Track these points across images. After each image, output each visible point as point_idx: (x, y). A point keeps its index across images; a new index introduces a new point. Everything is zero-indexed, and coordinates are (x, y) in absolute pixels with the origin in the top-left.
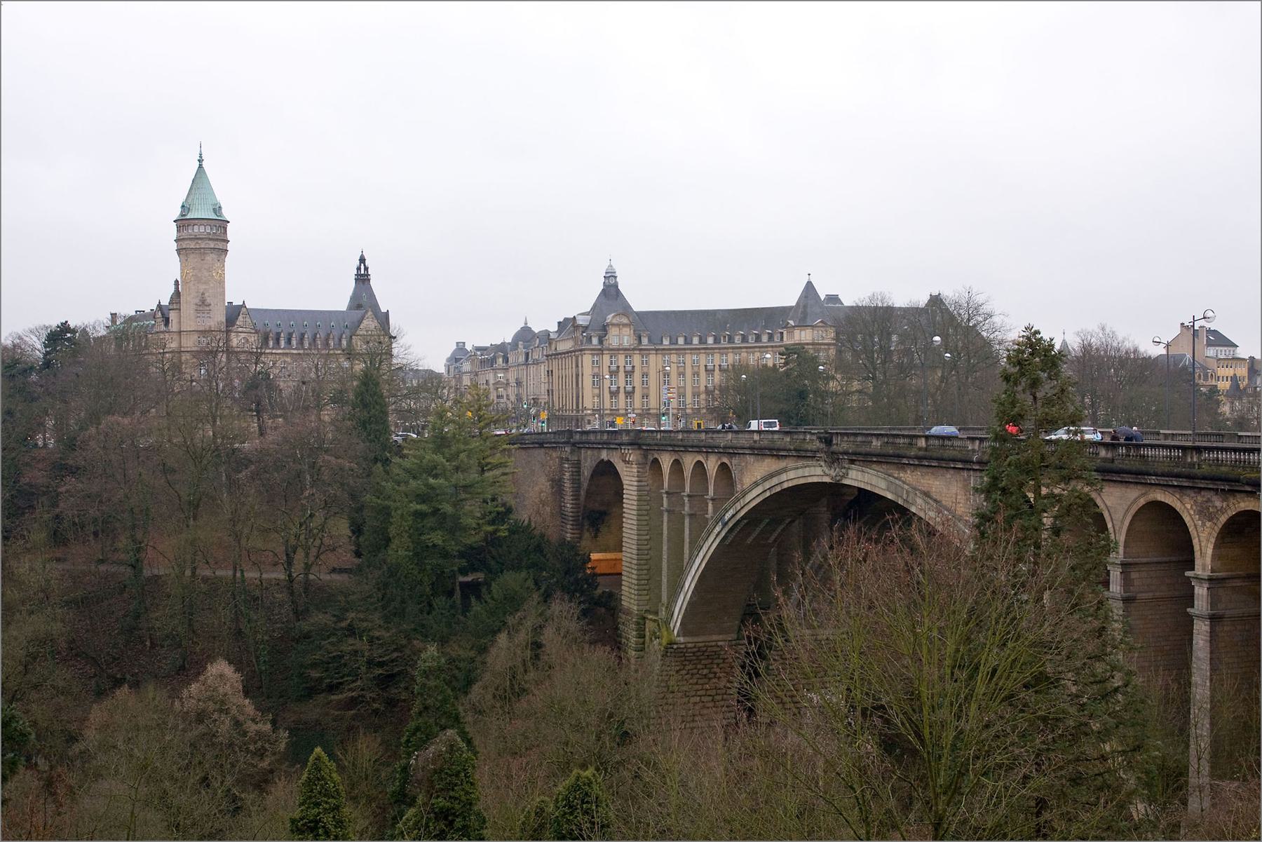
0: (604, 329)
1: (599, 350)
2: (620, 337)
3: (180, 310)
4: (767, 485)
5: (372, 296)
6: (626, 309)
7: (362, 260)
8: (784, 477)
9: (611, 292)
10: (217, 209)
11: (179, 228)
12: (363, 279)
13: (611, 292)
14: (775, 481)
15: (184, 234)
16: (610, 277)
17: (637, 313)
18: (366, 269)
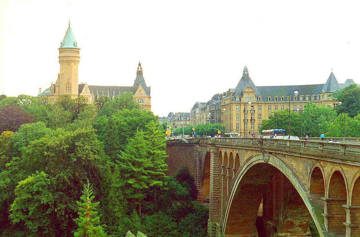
0: (242, 94)
1: (239, 103)
2: (249, 98)
3: (59, 86)
4: (248, 164)
5: (143, 81)
6: (252, 86)
7: (140, 65)
8: (252, 160)
9: (246, 78)
10: (75, 44)
11: (60, 52)
12: (140, 73)
13: (246, 78)
14: (250, 162)
15: (62, 55)
16: (246, 70)
17: (257, 87)
18: (141, 68)
